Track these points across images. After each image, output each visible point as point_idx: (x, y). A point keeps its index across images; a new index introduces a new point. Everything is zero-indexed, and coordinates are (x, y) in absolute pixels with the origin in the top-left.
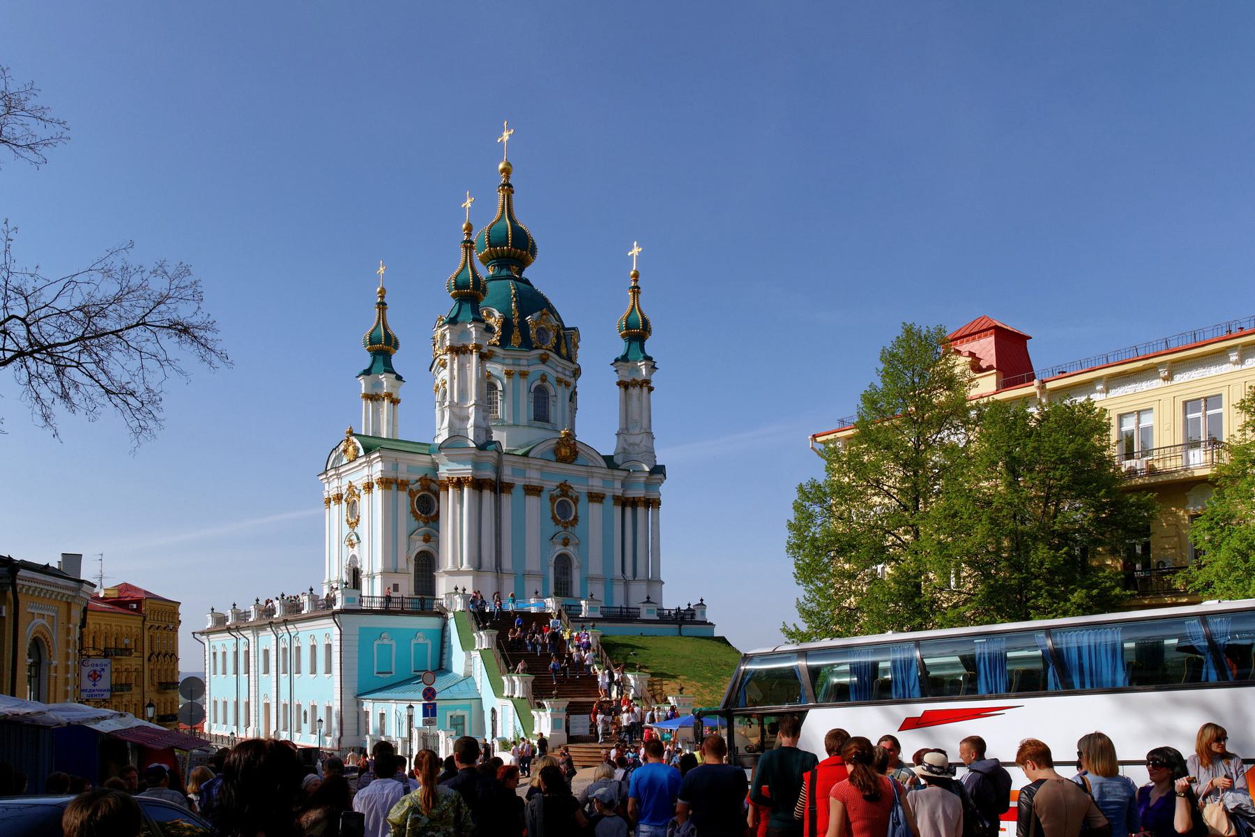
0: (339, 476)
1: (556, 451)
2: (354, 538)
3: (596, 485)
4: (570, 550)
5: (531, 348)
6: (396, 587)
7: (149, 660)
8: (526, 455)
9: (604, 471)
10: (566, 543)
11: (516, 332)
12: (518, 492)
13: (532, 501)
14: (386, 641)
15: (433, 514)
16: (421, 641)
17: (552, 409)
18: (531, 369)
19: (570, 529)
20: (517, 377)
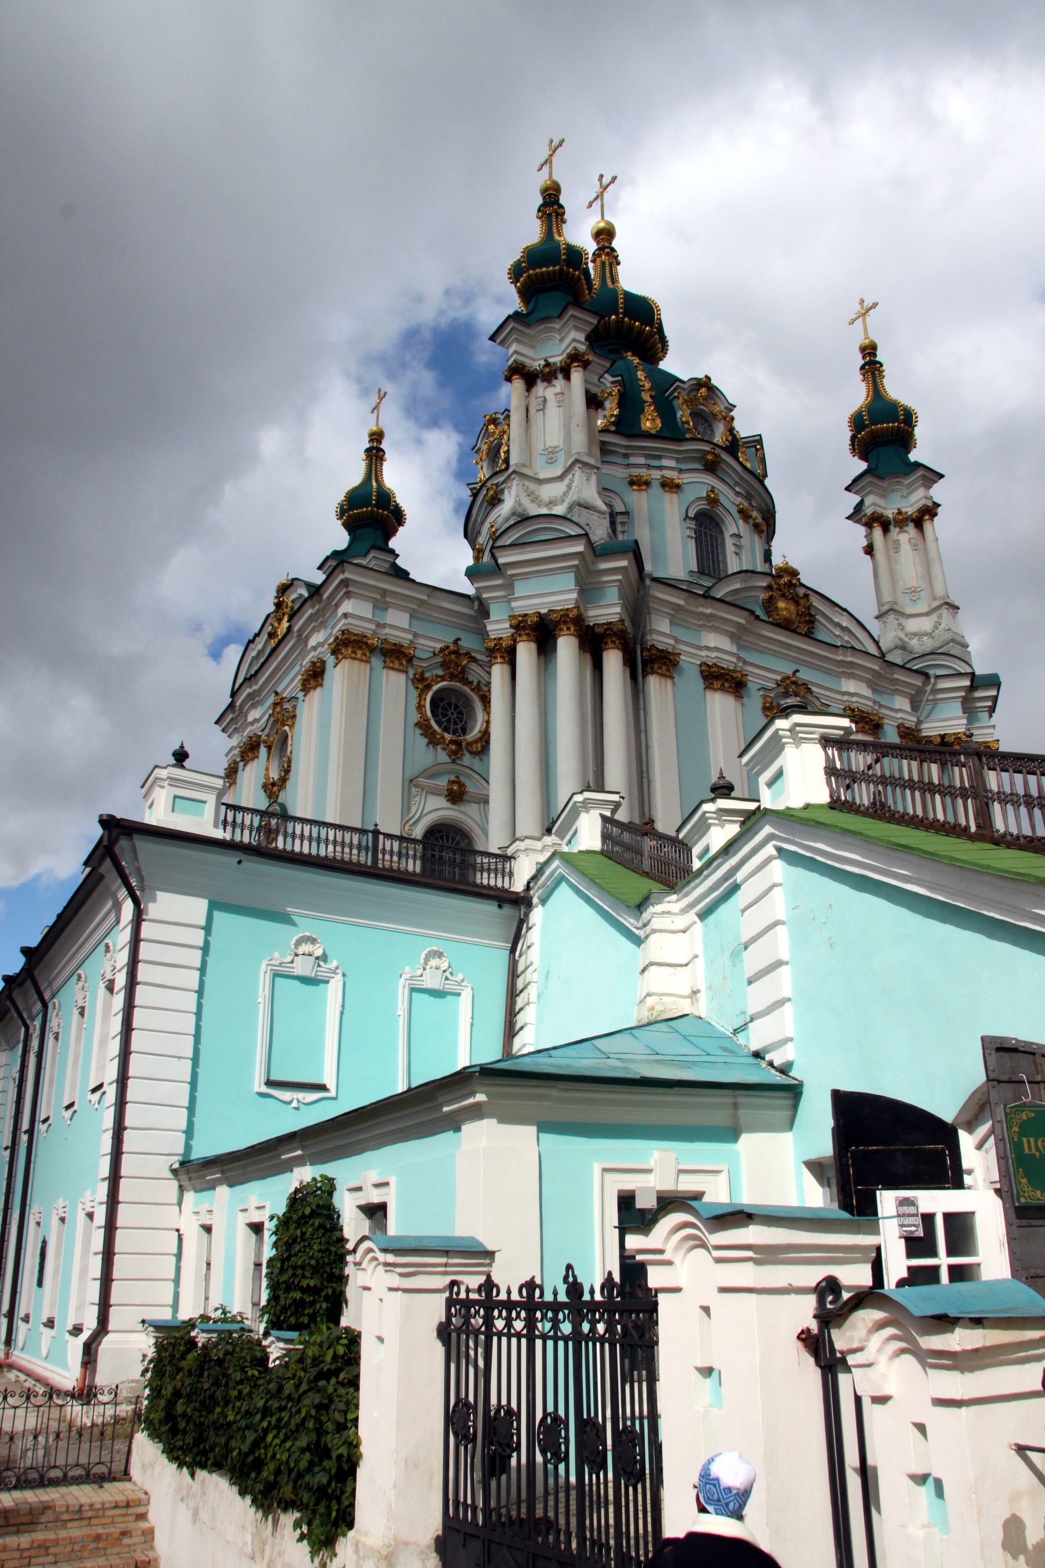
0: (254, 700)
1: (769, 605)
5: (680, 440)
11: (650, 409)
20: (656, 489)
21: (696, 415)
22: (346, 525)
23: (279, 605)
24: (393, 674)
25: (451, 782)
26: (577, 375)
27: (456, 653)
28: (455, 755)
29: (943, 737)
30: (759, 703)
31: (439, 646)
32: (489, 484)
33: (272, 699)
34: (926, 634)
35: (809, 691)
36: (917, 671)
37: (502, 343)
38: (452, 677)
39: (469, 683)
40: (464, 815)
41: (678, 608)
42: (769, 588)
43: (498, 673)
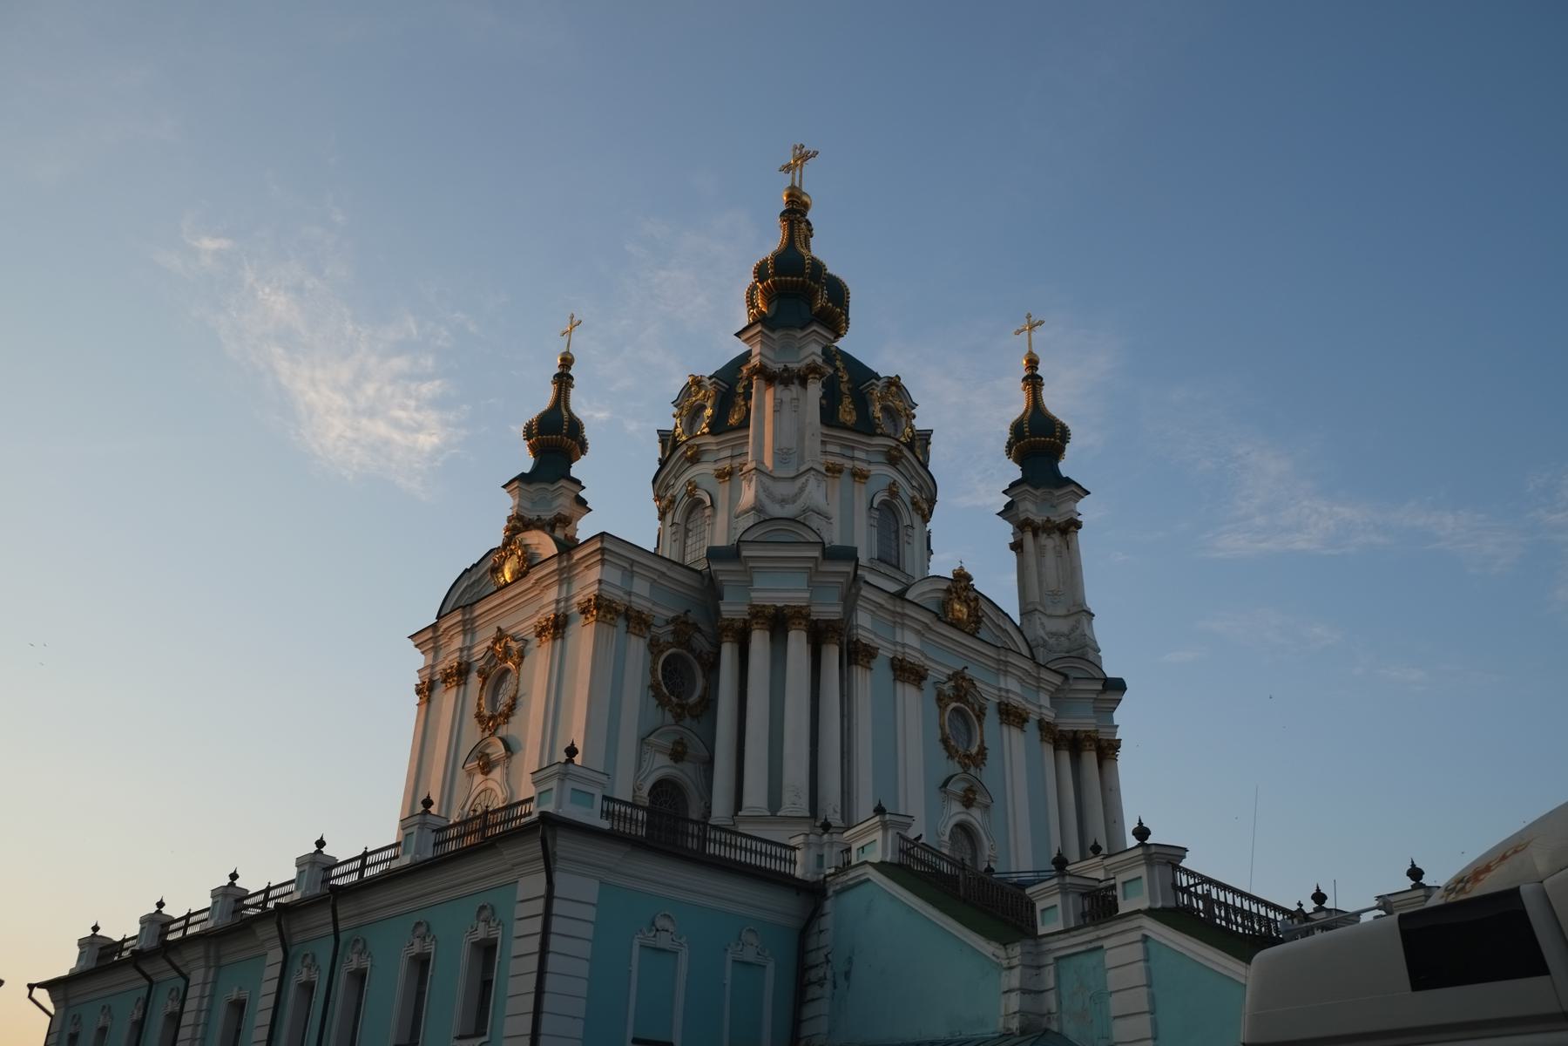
1: (945, 605)
2: (497, 750)
3: (1012, 688)
4: (975, 817)
5: (873, 434)
8: (900, 596)
9: (1027, 665)
10: (968, 802)
11: (847, 401)
14: (664, 941)
15: (693, 699)
16: (750, 955)
18: (875, 470)
19: (972, 770)
20: (846, 478)
21: (885, 409)
22: (531, 447)
23: (505, 545)
24: (633, 638)
25: (676, 743)
27: (685, 623)
28: (678, 718)
29: (1075, 732)
30: (934, 694)
32: (691, 442)
33: (491, 632)
34: (1063, 635)
36: (1055, 671)
37: (745, 341)
38: (679, 644)
39: (692, 651)
40: (685, 773)
41: (881, 606)
42: (948, 591)
43: (728, 652)
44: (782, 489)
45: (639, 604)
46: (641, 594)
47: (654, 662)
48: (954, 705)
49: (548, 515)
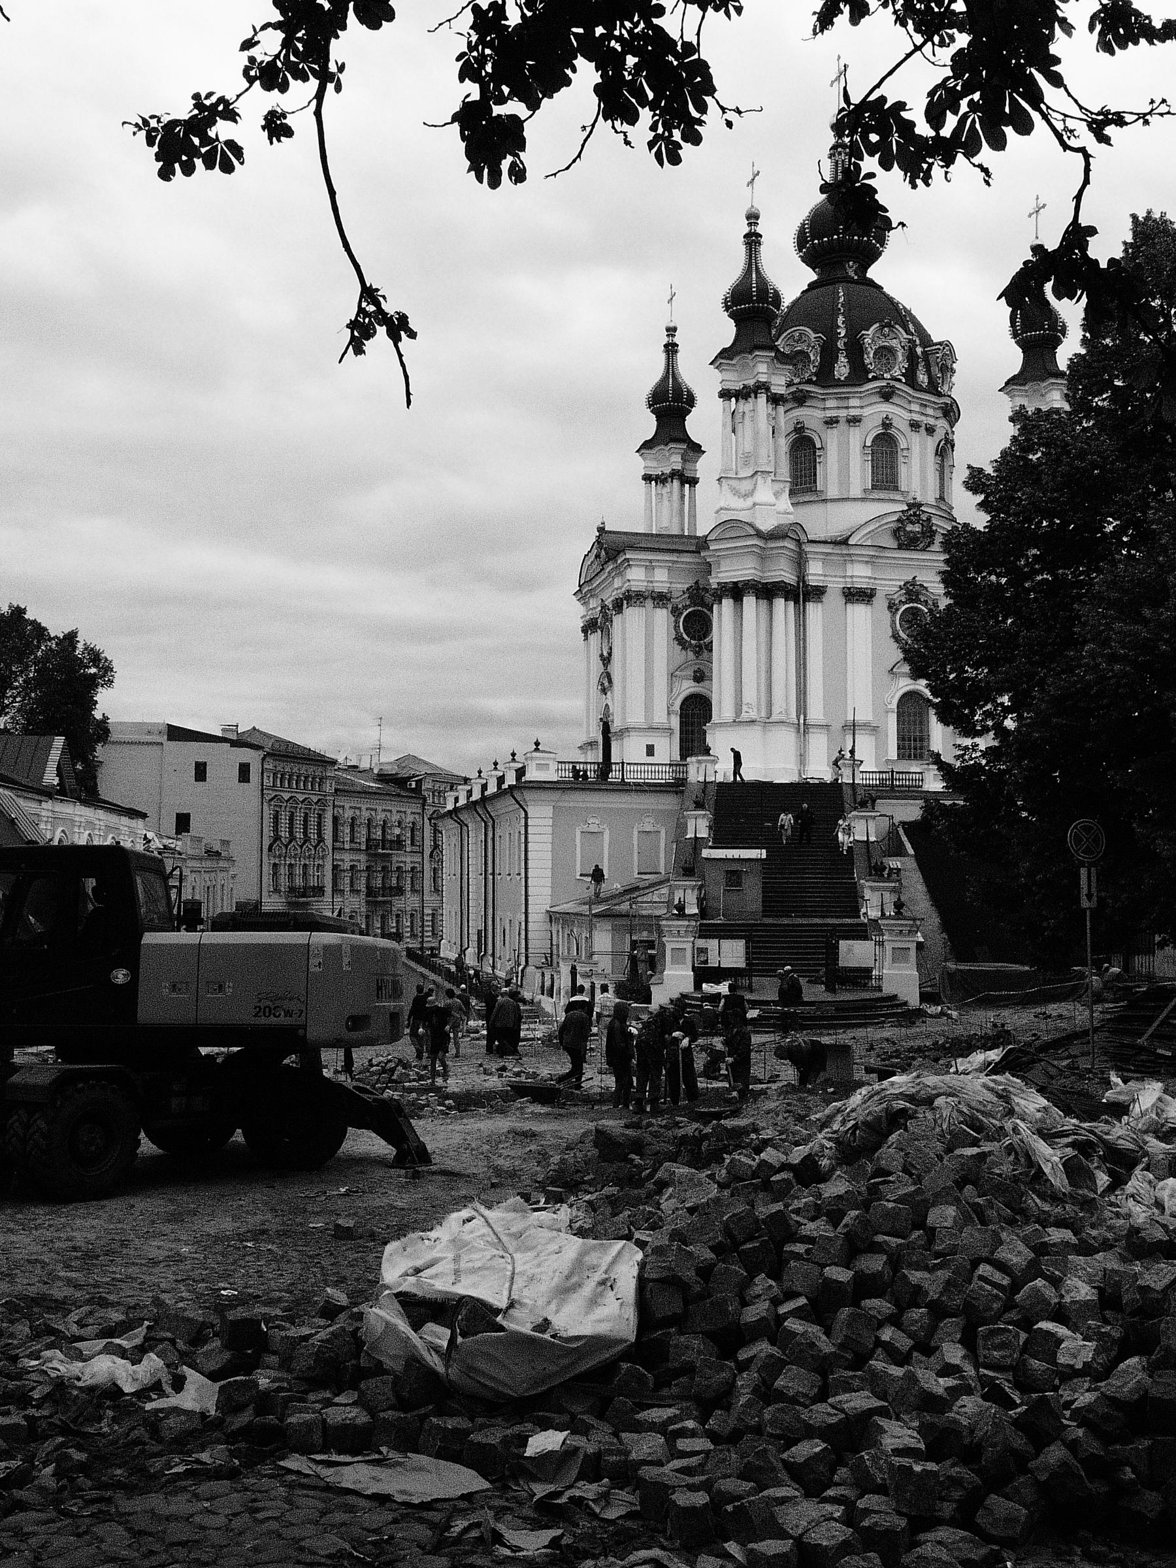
0: (592, 594)
1: (896, 533)
6: (650, 750)
7: (431, 856)
8: (844, 542)
11: (842, 359)
12: (833, 598)
13: (859, 613)
14: (593, 828)
17: (903, 470)
20: (843, 425)
25: (695, 672)
26: (762, 399)
27: (698, 589)
31: (687, 586)
35: (926, 588)
41: (828, 554)
42: (898, 520)
44: (746, 486)
45: (661, 587)
46: (661, 579)
47: (677, 622)
48: (907, 606)
49: (668, 471)
